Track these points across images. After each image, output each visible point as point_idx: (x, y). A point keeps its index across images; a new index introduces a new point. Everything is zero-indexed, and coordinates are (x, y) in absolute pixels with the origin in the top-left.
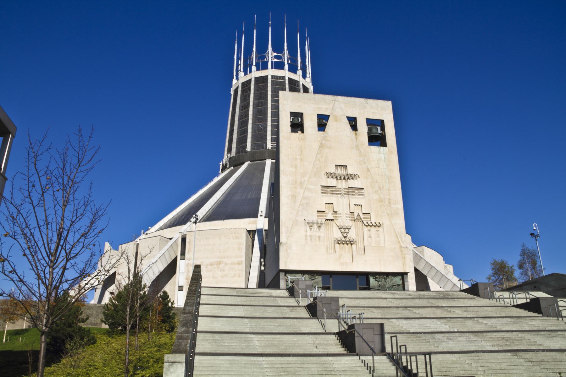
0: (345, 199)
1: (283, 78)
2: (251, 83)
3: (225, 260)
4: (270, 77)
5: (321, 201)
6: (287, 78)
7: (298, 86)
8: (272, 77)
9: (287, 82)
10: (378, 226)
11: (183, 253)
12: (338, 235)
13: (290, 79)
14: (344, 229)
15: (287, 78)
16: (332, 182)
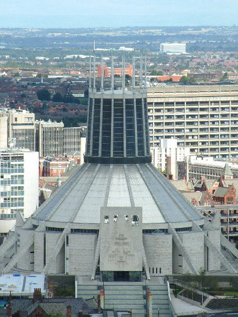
0: (121, 247)
1: (122, 100)
2: (100, 102)
3: (86, 248)
4: (113, 101)
5: (114, 248)
6: (124, 100)
7: (133, 103)
8: (115, 100)
9: (124, 104)
10: (133, 255)
11: (67, 243)
12: (119, 259)
13: (127, 100)
14: (121, 257)
15: (124, 100)
16: (118, 241)
